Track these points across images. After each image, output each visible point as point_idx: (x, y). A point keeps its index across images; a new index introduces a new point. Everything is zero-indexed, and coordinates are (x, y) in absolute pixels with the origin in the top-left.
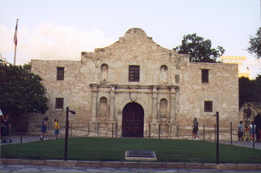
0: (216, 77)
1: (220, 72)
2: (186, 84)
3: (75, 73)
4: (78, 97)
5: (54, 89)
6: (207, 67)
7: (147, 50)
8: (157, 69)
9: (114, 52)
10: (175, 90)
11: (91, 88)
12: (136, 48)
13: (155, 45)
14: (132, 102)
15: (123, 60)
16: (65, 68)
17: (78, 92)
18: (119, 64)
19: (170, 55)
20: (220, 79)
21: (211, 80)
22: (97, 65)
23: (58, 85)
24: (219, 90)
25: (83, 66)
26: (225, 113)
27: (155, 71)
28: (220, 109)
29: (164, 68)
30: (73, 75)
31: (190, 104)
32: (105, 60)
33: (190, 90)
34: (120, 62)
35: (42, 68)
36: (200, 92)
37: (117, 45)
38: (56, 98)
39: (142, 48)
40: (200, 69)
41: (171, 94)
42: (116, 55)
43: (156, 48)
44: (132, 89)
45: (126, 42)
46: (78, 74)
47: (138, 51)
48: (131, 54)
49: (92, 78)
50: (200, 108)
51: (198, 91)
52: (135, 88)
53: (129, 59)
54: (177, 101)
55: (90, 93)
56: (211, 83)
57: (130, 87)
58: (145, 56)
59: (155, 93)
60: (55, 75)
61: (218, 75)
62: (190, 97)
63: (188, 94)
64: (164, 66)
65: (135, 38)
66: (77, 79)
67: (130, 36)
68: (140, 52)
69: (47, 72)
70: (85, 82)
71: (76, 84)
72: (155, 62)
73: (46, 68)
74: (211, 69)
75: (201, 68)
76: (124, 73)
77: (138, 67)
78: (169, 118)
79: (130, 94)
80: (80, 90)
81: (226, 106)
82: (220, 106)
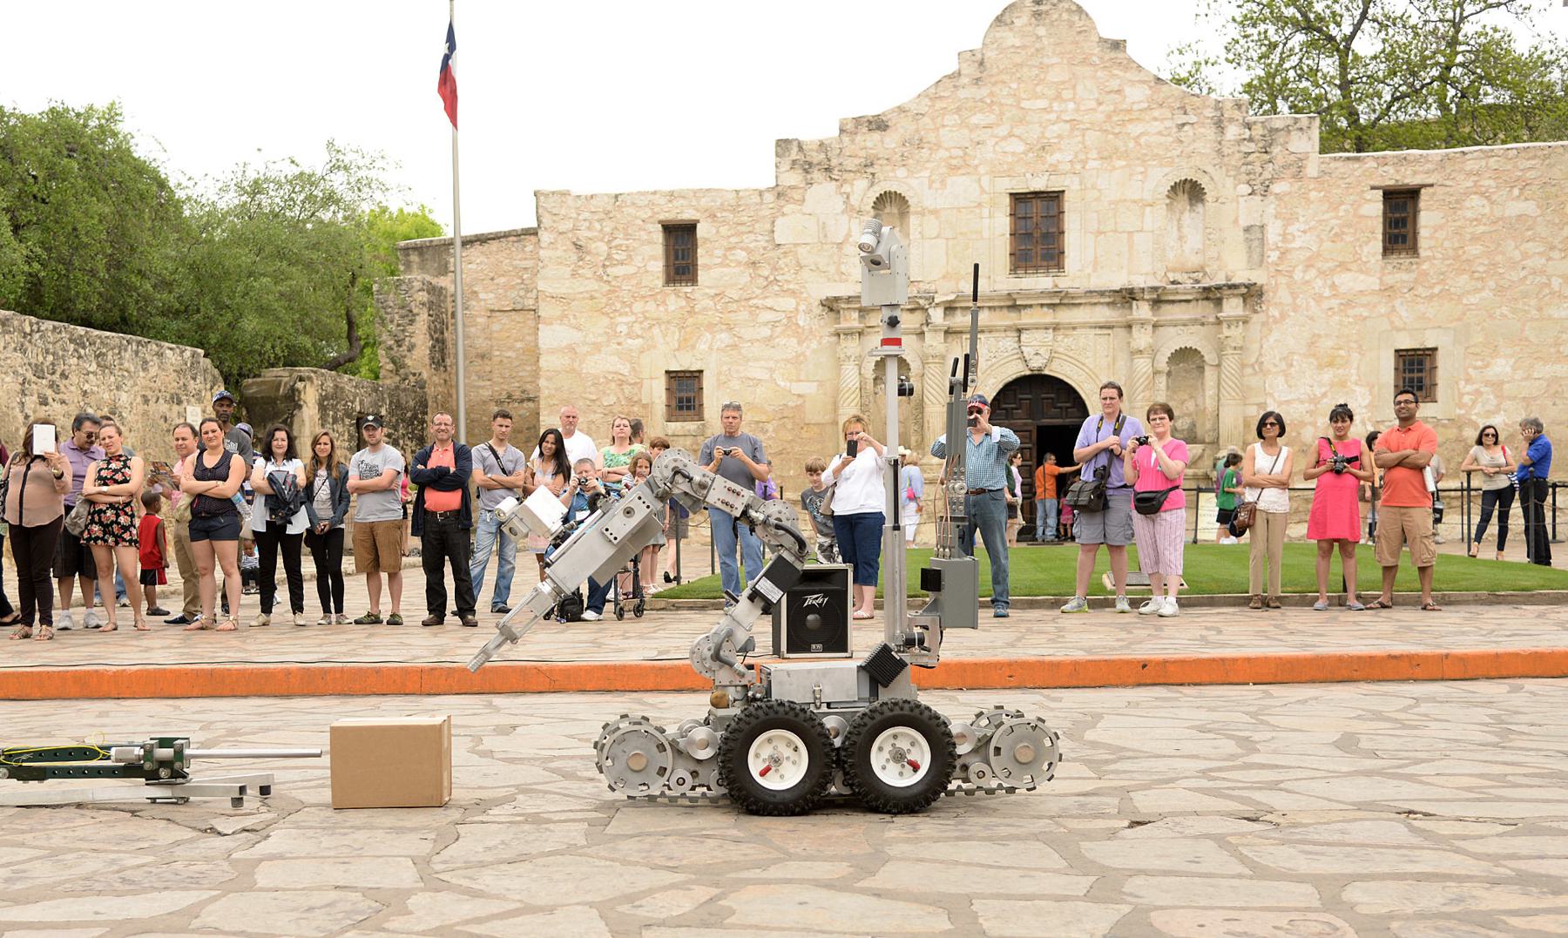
0: (1458, 224)
1: (1482, 194)
2: (1300, 267)
3: (751, 245)
4: (771, 364)
5: (656, 330)
6: (1415, 173)
7: (1102, 108)
8: (1150, 202)
10: (1244, 301)
11: (832, 315)
12: (1041, 104)
14: (1028, 373)
15: (982, 170)
16: (699, 226)
17: (770, 338)
18: (962, 188)
19: (1220, 125)
20: (1481, 229)
21: (1432, 243)
22: (854, 200)
23: (671, 308)
24: (1477, 290)
25: (788, 208)
26: (1507, 404)
27: (1143, 214)
28: (1475, 386)
29: (1186, 196)
30: (741, 255)
31: (1320, 367)
32: (891, 174)
33: (1319, 298)
35: (589, 228)
36: (1375, 306)
38: (667, 372)
39: (1073, 99)
40: (1373, 188)
41: (1225, 325)
43: (1148, 92)
44: (1028, 311)
45: (991, 76)
46: (765, 249)
47: (1053, 116)
49: (832, 269)
50: (1371, 387)
51: (1364, 300)
53: (1010, 160)
54: (1253, 360)
55: (825, 340)
56: (1434, 258)
58: (1092, 137)
59: (1143, 324)
60: (656, 260)
61: (1469, 214)
62: (1319, 336)
63: (1311, 319)
64: (1188, 186)
65: (1037, 50)
68: (1067, 121)
69: (618, 247)
70: (797, 287)
72: (1142, 169)
73: (607, 230)
74: (1432, 185)
75: (1377, 183)
76: (986, 235)
77: (1055, 197)
78: (1213, 443)
80: (779, 330)
81: (1508, 369)
82: (1475, 368)
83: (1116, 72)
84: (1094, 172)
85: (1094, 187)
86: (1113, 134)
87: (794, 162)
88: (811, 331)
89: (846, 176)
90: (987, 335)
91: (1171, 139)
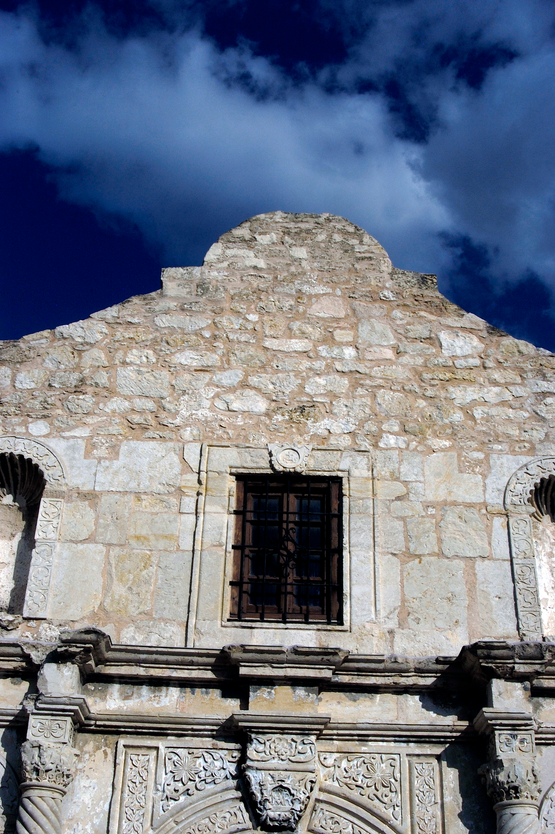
9: (109, 368)
12: (298, 345)
13: (463, 328)
15: (187, 434)
32: (23, 430)
34: (152, 444)
37: (135, 320)
42: (127, 392)
47: (318, 365)
48: (257, 389)
52: (295, 682)
53: (240, 422)
57: (243, 671)
65: (294, 275)
67: (248, 263)
79: (243, 751)
83: (422, 313)
84: (395, 454)
85: (395, 477)
86: (425, 397)
90: (172, 741)
91: (527, 415)
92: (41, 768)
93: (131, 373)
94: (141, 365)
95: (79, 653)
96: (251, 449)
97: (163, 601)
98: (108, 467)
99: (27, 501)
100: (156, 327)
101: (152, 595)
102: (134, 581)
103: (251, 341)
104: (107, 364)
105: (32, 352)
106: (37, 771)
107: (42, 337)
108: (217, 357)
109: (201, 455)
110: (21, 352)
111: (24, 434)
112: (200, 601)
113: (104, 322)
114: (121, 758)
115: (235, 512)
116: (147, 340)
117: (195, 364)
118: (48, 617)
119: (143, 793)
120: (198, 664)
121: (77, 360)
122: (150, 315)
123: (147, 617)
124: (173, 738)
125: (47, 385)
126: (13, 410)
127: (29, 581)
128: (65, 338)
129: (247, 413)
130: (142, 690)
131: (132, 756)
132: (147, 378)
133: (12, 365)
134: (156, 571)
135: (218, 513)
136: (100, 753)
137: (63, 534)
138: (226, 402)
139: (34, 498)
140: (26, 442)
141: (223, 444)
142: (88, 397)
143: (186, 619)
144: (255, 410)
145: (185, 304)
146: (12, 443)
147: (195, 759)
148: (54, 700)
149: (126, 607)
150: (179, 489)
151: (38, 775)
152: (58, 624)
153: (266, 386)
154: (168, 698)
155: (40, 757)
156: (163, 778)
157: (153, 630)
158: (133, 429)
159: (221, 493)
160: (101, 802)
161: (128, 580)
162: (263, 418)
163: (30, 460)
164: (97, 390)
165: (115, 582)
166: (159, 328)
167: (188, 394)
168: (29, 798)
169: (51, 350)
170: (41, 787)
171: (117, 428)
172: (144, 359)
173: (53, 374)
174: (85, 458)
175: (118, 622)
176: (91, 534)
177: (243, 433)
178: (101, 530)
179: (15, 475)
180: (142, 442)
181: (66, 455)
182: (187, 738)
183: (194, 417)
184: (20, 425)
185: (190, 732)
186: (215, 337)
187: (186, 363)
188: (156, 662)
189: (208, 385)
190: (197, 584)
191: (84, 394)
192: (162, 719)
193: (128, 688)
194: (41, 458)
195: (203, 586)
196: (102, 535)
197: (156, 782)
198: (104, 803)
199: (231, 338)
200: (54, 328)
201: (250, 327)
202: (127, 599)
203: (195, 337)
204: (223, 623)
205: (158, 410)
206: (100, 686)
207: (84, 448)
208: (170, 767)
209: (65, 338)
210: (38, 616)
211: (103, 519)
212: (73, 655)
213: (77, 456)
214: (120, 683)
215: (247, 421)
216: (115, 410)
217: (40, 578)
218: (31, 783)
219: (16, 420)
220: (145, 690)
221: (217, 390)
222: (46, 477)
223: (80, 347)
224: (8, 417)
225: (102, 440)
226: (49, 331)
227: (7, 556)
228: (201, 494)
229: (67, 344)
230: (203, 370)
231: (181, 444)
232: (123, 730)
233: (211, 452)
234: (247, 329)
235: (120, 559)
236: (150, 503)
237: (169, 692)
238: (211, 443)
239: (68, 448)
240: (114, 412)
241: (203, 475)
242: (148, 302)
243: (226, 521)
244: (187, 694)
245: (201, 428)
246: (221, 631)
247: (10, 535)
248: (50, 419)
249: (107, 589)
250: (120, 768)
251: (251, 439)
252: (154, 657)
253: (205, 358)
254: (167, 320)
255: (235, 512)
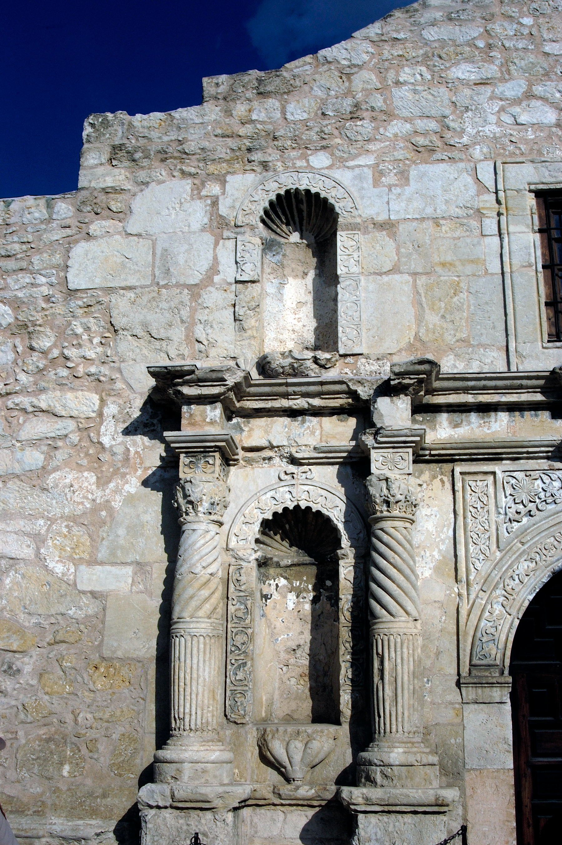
3: (20, 294)
15: (477, 152)
17: (44, 471)
22: (223, 210)
34: (443, 166)
37: (401, 36)
42: (405, 113)
46: (48, 299)
66: (32, 349)
71: (25, 401)
80: (60, 455)
87: (116, 149)
88: (127, 459)
89: (212, 168)
90: (507, 465)
92: (392, 499)
93: (406, 93)
94: (415, 83)
95: (413, 384)
96: (547, 164)
97: (479, 327)
98: (400, 194)
99: (315, 238)
100: (425, 41)
101: (467, 321)
102: (446, 309)
103: (529, 47)
104: (380, 86)
105: (297, 80)
106: (388, 503)
107: (305, 64)
108: (496, 68)
109: (496, 174)
110: (285, 81)
111: (306, 167)
112: (518, 324)
113: (368, 41)
114: (459, 485)
115: (540, 231)
116: (418, 56)
117: (473, 77)
118: (365, 351)
119: (486, 517)
120: (527, 387)
121: (347, 84)
122: (416, 28)
123: (464, 344)
124: (508, 462)
125: (320, 114)
126: (289, 144)
127: (339, 317)
128: (330, 63)
129: (537, 126)
130: (471, 417)
131: (470, 483)
132: (425, 97)
133: (279, 97)
134: (467, 297)
135: (523, 232)
136: (437, 482)
137: (365, 267)
138: (513, 115)
139: (323, 234)
140: (310, 175)
141: (518, 160)
142: (366, 123)
143: (505, 344)
144: (545, 121)
145: (452, 13)
146: (295, 178)
147: (533, 481)
148: (395, 432)
149: (442, 335)
150: (478, 211)
151: (389, 506)
152: (376, 358)
153: (553, 95)
154: (498, 423)
155: (388, 489)
156: (503, 501)
157: (473, 356)
158: (419, 152)
159: (523, 211)
160: (445, 529)
161: (440, 308)
162: (554, 129)
163: (317, 194)
164: (374, 114)
165: (427, 311)
166: (428, 42)
167: (472, 110)
168: (382, 529)
169: (317, 77)
170: (394, 518)
171: (402, 152)
172: (419, 77)
173: (324, 102)
174: (374, 187)
175: (437, 352)
176: (395, 265)
177: (535, 147)
178: (404, 260)
179: (300, 211)
180: (431, 165)
181: (353, 185)
182: (522, 461)
183: (481, 134)
184: (299, 158)
185: (525, 455)
186: (490, 47)
187: (463, 77)
188: (485, 388)
189: (491, 98)
190: (512, 307)
191: (361, 120)
192: (497, 444)
193: (456, 416)
194: (328, 191)
195: (518, 309)
196: (406, 265)
197: (497, 506)
198: (448, 530)
199: (507, 45)
200: (316, 52)
201: (526, 31)
202: (442, 328)
203: (468, 49)
204: (544, 345)
205: (442, 130)
206: (428, 416)
207: (371, 176)
208: (509, 491)
209: (330, 63)
210: (355, 352)
211: (405, 248)
212: (406, 387)
213: (365, 185)
214: (448, 412)
215: (538, 133)
216: (397, 134)
217: (350, 314)
218: (382, 515)
219: (295, 153)
220: (473, 416)
221: (501, 103)
222: (337, 210)
223: (348, 70)
224: (286, 151)
225: (389, 167)
226: (311, 56)
227: (303, 295)
228: (503, 214)
229: (333, 68)
230: (483, 83)
231: (472, 164)
232: (458, 457)
233: (506, 170)
234: (522, 34)
235: (429, 288)
236: (450, 228)
237: (498, 417)
238: (504, 160)
239: (355, 178)
240: (396, 135)
241: (501, 194)
242: (411, 14)
243: (532, 241)
244: (517, 418)
245: (491, 145)
246: (543, 353)
247: (302, 274)
248: (330, 149)
249: (420, 319)
250: (459, 495)
251: (545, 153)
252: (483, 383)
253: (483, 70)
254: (436, 32)
255: (540, 231)
